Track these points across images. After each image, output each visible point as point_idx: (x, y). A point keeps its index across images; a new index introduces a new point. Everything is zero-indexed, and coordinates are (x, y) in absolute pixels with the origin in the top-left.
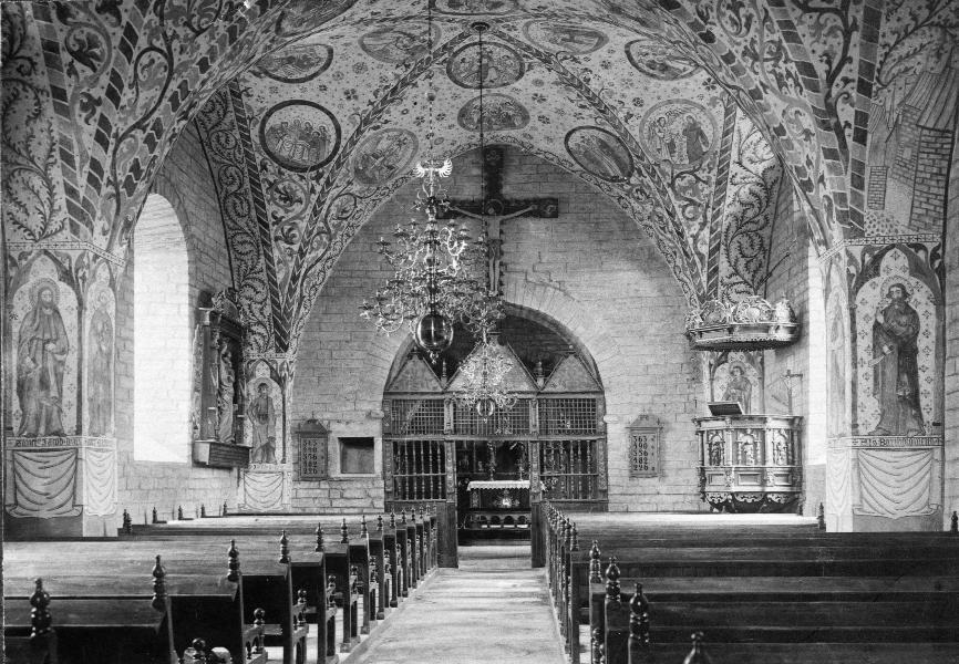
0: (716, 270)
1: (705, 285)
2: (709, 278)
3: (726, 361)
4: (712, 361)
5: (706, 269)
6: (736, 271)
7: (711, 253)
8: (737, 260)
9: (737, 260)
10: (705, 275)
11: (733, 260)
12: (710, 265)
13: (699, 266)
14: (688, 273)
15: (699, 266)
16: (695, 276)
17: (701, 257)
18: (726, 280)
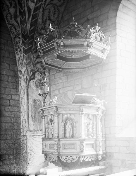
0: (36, 21)
1: (28, 29)
2: (31, 26)
3: (34, 79)
4: (28, 78)
5: (30, 19)
6: (44, 25)
7: (36, 9)
8: (46, 20)
9: (46, 20)
10: (30, 22)
11: (44, 19)
12: (33, 18)
13: (27, 15)
14: (19, 19)
15: (27, 15)
16: (23, 22)
17: (29, 10)
18: (39, 30)
